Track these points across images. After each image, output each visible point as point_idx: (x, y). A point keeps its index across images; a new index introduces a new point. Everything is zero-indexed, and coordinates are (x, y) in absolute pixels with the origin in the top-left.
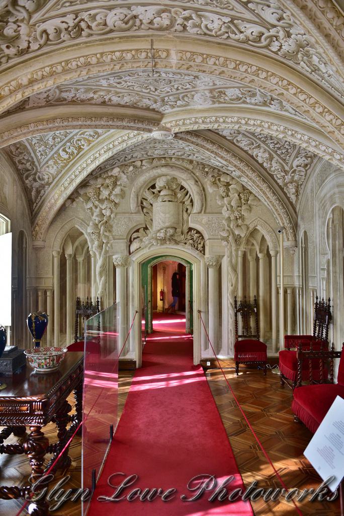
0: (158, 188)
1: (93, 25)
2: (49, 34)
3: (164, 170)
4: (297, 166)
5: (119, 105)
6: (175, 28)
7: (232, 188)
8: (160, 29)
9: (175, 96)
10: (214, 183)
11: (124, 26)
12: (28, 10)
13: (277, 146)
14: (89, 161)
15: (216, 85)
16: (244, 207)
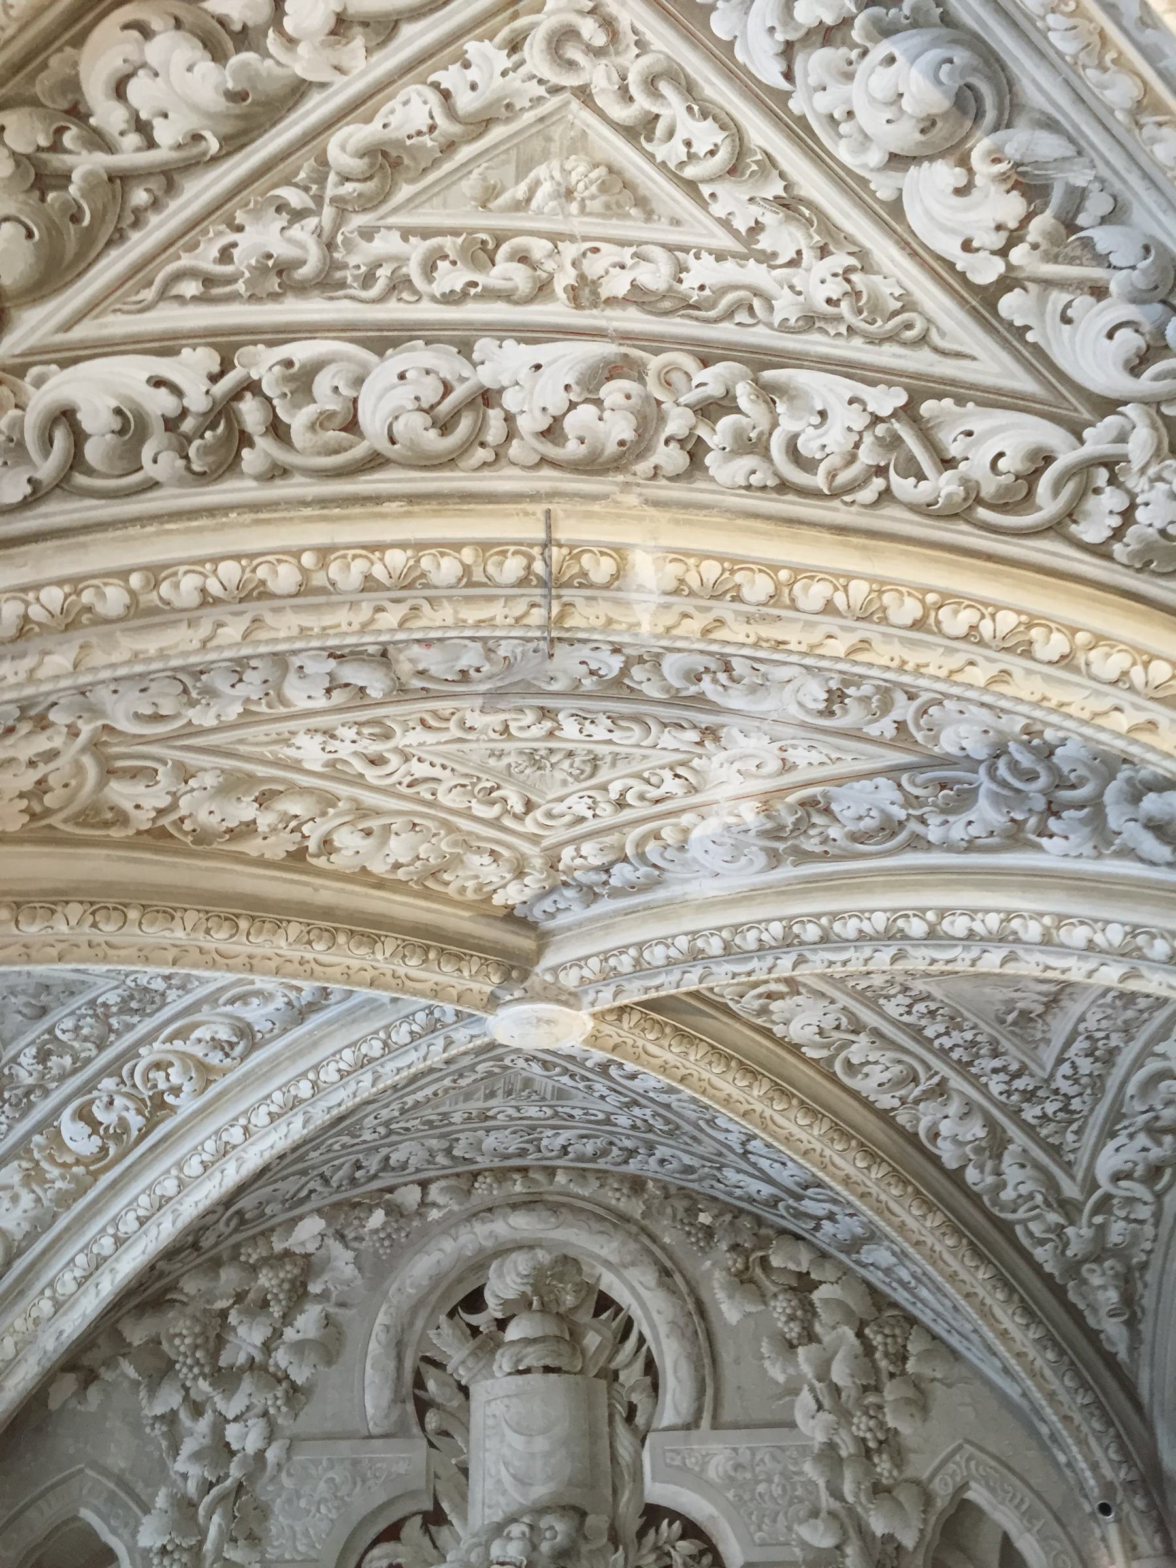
0: (494, 1309)
1: (298, 420)
2: (87, 436)
3: (522, 1224)
4: (1117, 1177)
5: (363, 876)
6: (652, 460)
7: (826, 1301)
8: (592, 465)
9: (611, 839)
10: (743, 1280)
11: (432, 440)
13: (1019, 1084)
14: (193, 1167)
15: (794, 766)
16: (891, 1392)
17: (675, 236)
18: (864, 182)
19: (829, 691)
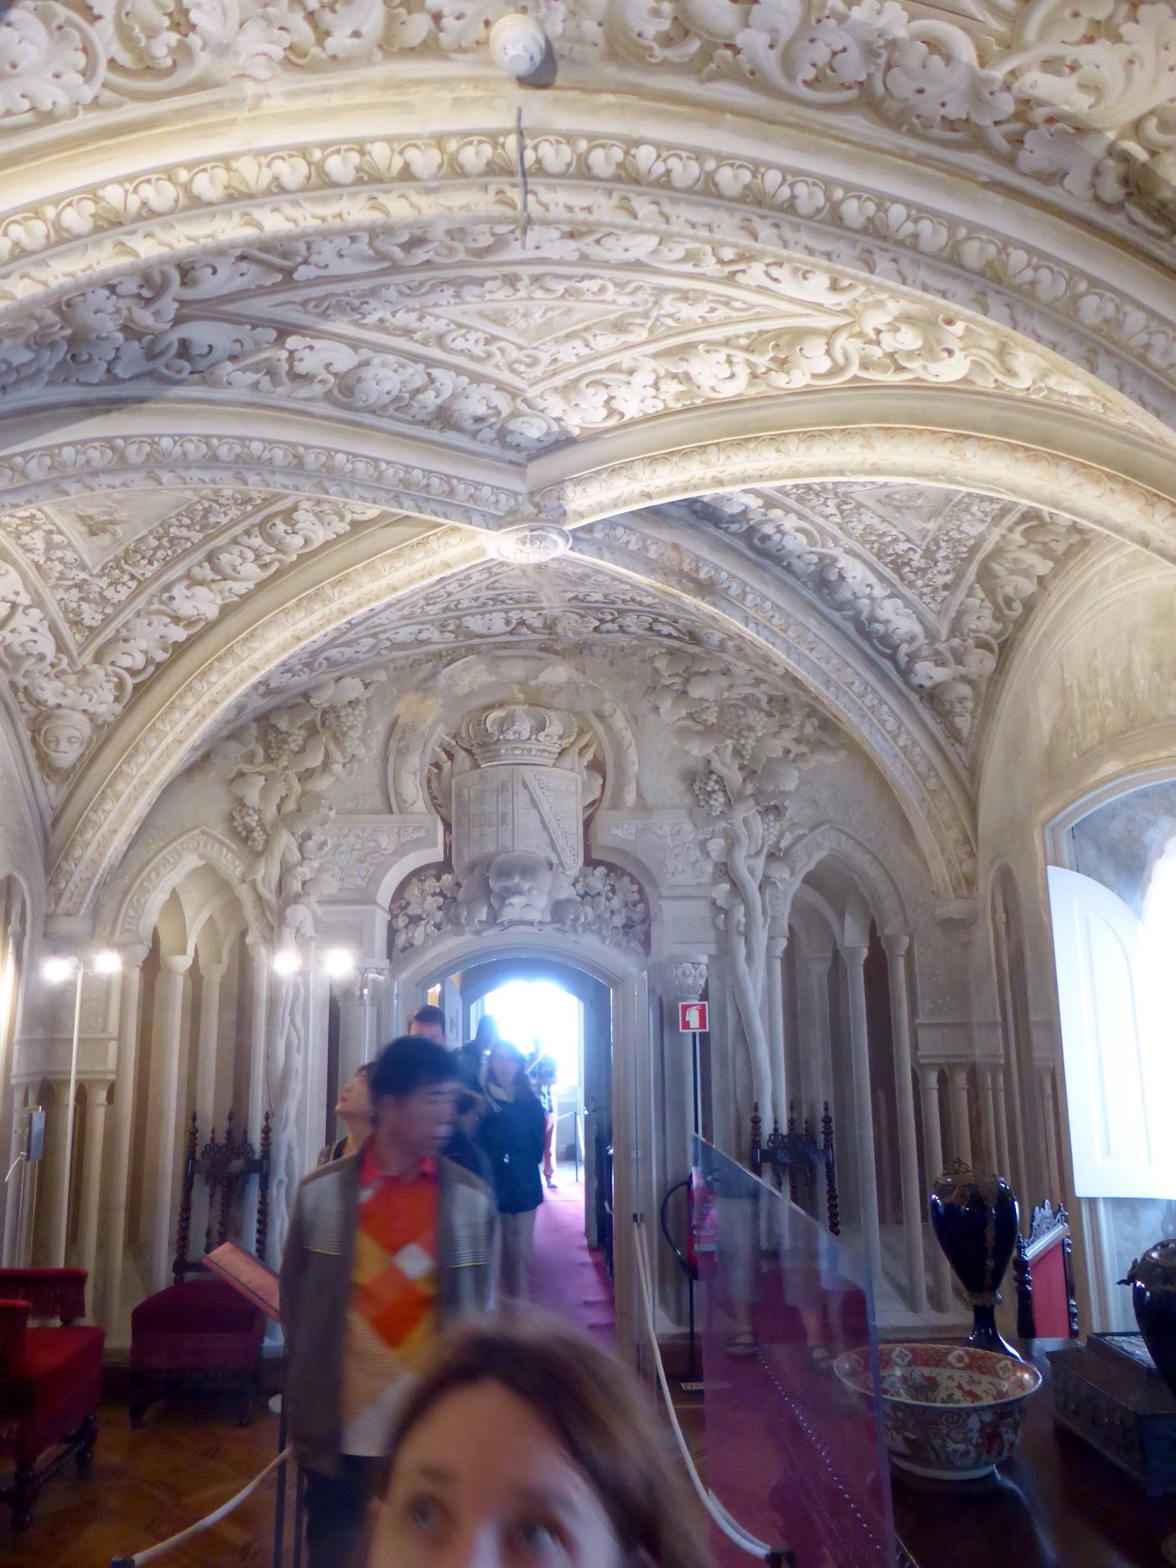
19: (193, 27)
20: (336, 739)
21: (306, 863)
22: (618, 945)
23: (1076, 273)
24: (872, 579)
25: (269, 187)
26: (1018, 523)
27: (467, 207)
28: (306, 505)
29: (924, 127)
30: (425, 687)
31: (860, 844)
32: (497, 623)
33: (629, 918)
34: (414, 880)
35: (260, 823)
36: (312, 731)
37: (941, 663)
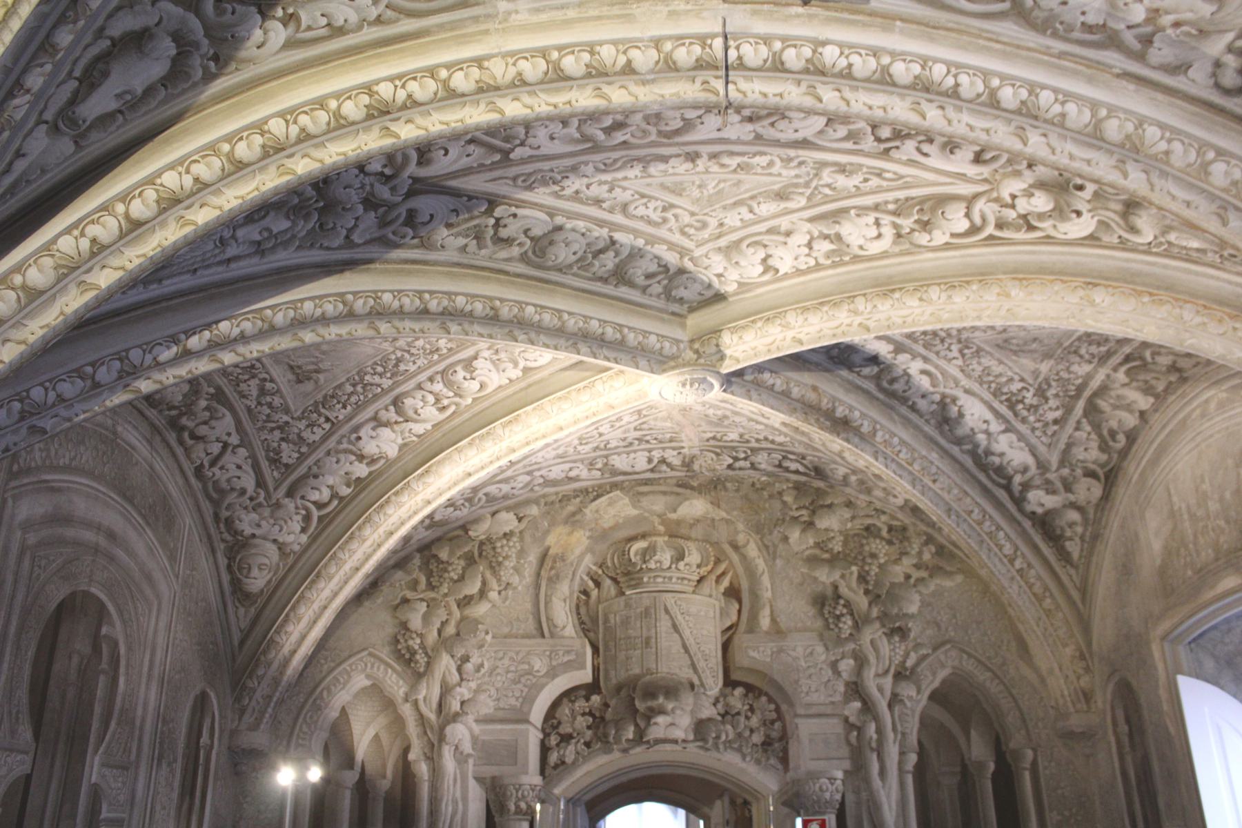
12: (967, 208)
17: (649, 180)
18: (568, 218)
20: (492, 568)
21: (464, 683)
22: (758, 762)
23: (1203, 146)
24: (989, 416)
25: (514, 79)
26: (1121, 364)
27: (677, 94)
28: (486, 354)
29: (1065, 31)
30: (573, 521)
31: (979, 661)
32: (641, 463)
33: (767, 736)
34: (565, 700)
35: (423, 646)
36: (471, 561)
37: (1051, 491)
